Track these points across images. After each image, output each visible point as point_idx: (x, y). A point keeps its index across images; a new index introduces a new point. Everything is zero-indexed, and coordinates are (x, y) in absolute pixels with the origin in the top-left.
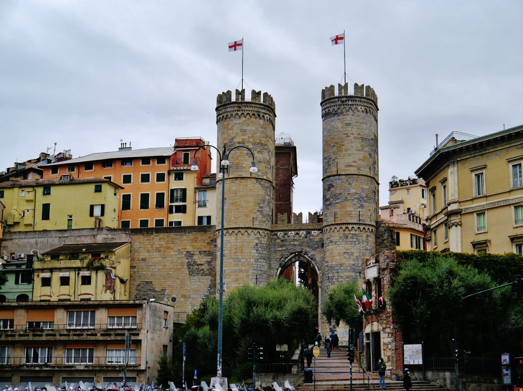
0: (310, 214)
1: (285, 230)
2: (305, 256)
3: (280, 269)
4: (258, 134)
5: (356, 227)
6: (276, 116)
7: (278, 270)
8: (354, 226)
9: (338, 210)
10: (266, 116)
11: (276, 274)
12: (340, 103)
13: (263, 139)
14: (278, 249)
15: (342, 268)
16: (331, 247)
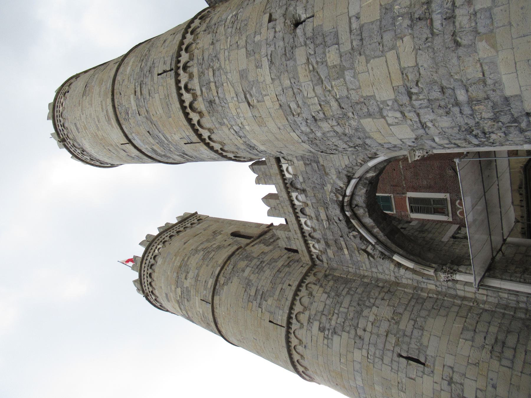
0: (258, 181)
1: (304, 236)
2: (348, 192)
3: (396, 258)
4: (169, 273)
5: (184, 78)
6: (196, 213)
7: (399, 265)
8: (182, 85)
9: (177, 137)
10: (156, 251)
11: (413, 271)
12: (70, 145)
13: (175, 264)
14: (348, 256)
15: (293, 106)
16: (262, 148)
